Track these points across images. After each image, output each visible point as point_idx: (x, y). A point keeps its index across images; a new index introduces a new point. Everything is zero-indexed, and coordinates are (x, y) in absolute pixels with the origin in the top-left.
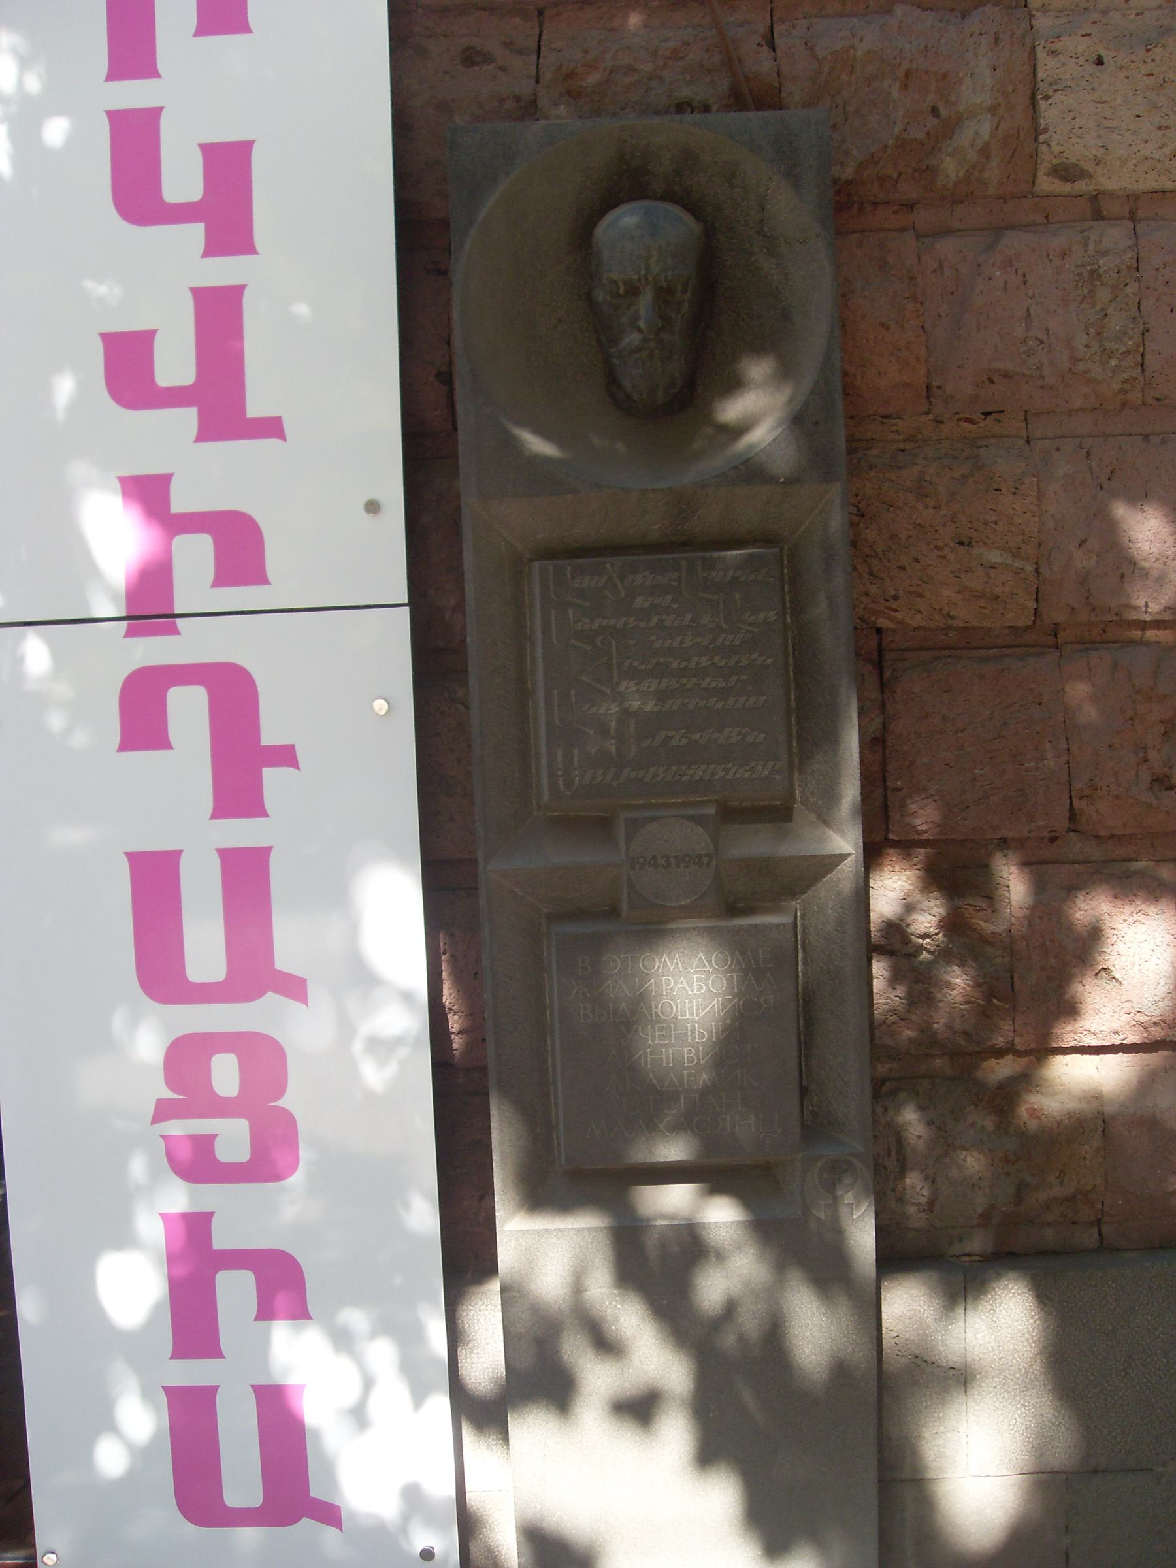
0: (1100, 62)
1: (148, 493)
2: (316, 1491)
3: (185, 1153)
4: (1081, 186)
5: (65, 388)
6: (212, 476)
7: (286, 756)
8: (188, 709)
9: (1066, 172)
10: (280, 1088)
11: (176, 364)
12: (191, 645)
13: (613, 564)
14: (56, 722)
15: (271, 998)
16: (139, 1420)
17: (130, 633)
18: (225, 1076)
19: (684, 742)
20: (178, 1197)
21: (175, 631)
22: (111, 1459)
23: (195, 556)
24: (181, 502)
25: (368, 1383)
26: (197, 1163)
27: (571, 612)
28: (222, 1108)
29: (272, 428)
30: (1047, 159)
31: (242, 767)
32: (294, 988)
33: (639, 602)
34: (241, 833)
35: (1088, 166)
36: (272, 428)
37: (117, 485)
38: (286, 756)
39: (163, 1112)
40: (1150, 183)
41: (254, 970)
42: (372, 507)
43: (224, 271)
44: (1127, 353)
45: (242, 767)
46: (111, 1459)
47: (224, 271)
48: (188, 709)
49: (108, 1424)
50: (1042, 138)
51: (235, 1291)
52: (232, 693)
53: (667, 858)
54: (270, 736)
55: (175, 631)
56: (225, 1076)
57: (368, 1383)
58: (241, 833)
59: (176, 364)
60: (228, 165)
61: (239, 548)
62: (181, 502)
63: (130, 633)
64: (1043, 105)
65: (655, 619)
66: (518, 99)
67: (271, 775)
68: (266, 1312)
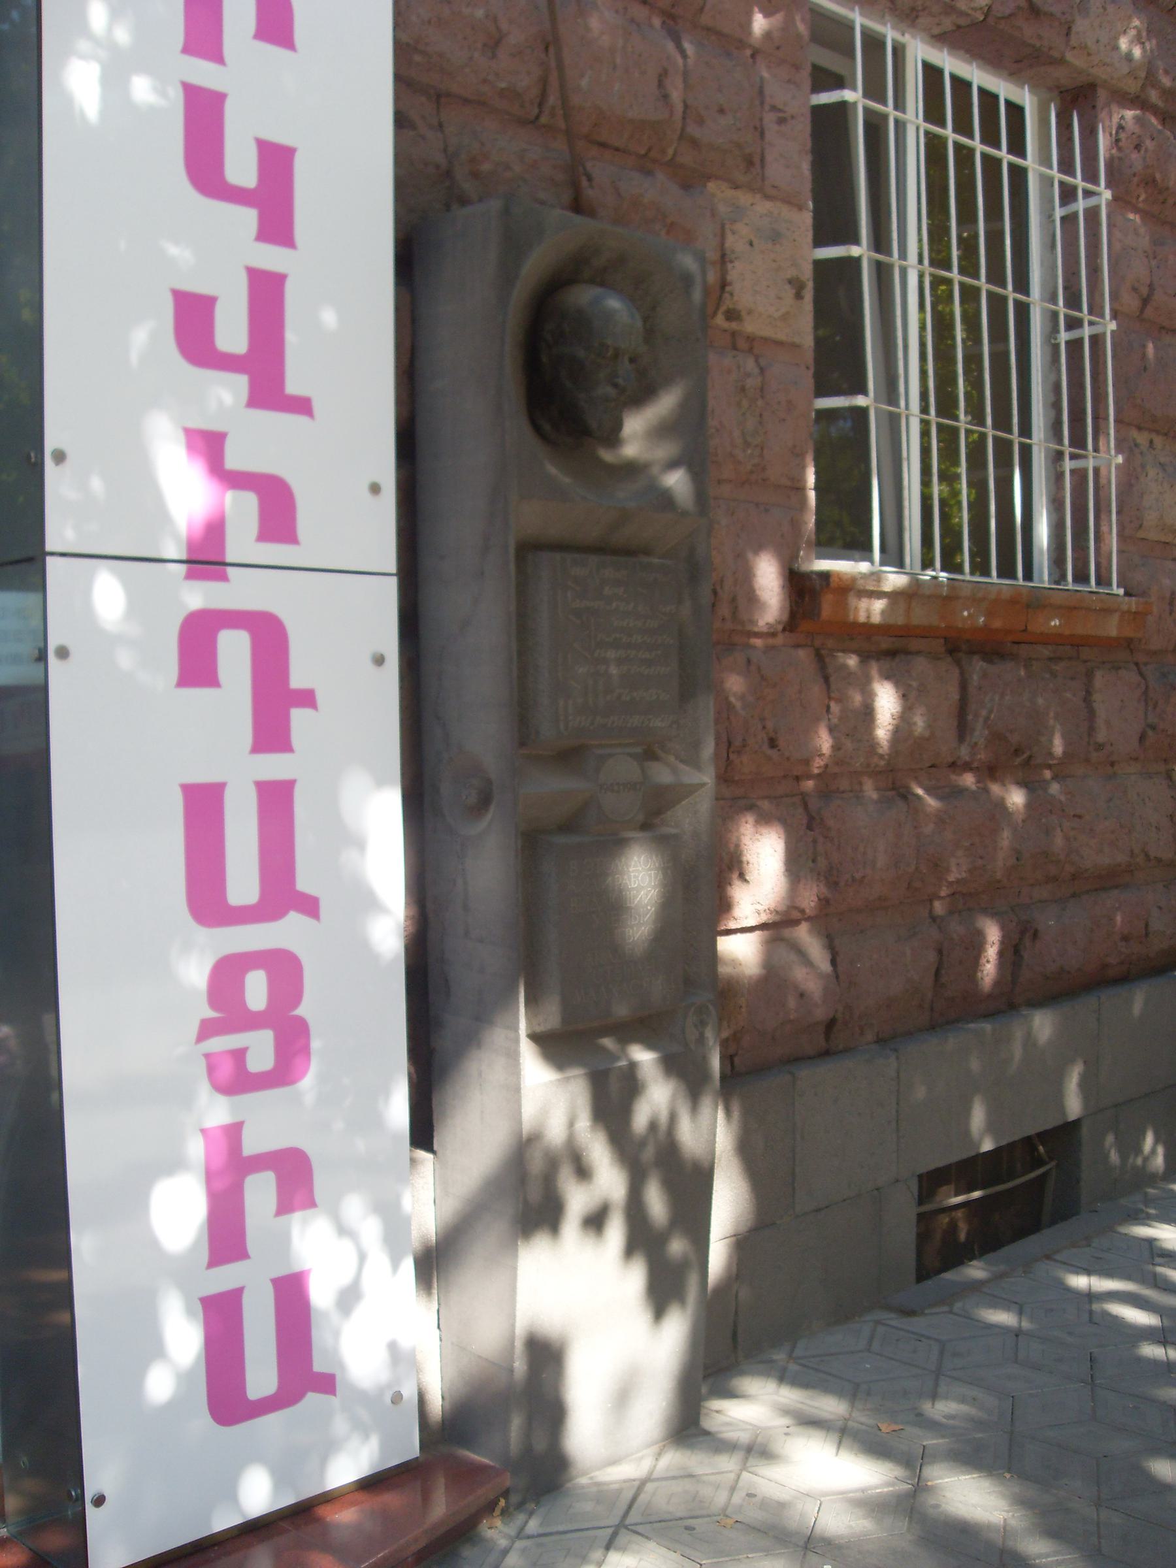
0: (751, 244)
1: (209, 446)
2: (319, 1365)
3: (226, 1070)
4: (734, 325)
5: (140, 337)
6: (261, 440)
7: (307, 699)
8: (234, 650)
9: (733, 315)
10: (296, 997)
11: (232, 332)
12: (238, 592)
13: (593, 560)
14: (125, 659)
15: (293, 917)
16: (184, 1339)
17: (190, 576)
18: (256, 990)
19: (628, 698)
20: (218, 1111)
21: (224, 578)
22: (160, 1385)
23: (243, 510)
24: (234, 461)
25: (362, 1257)
26: (236, 1079)
27: (569, 594)
28: (253, 1022)
29: (302, 406)
30: (727, 303)
31: (275, 709)
32: (310, 906)
33: (607, 591)
34: (274, 767)
35: (743, 313)
36: (302, 406)
37: (182, 437)
38: (307, 699)
39: (207, 1030)
40: (767, 332)
41: (282, 894)
42: (375, 489)
43: (271, 258)
44: (757, 446)
45: (275, 709)
46: (160, 1385)
47: (271, 258)
48: (234, 650)
49: (155, 1350)
50: (728, 289)
51: (260, 1192)
52: (269, 636)
53: (618, 784)
54: (298, 680)
55: (224, 578)
56: (256, 990)
57: (362, 1257)
58: (274, 767)
59: (232, 332)
60: (276, 160)
61: (278, 511)
62: (234, 461)
63: (190, 576)
64: (729, 266)
65: (614, 605)
66: (438, 167)
67: (299, 717)
68: (285, 1207)
